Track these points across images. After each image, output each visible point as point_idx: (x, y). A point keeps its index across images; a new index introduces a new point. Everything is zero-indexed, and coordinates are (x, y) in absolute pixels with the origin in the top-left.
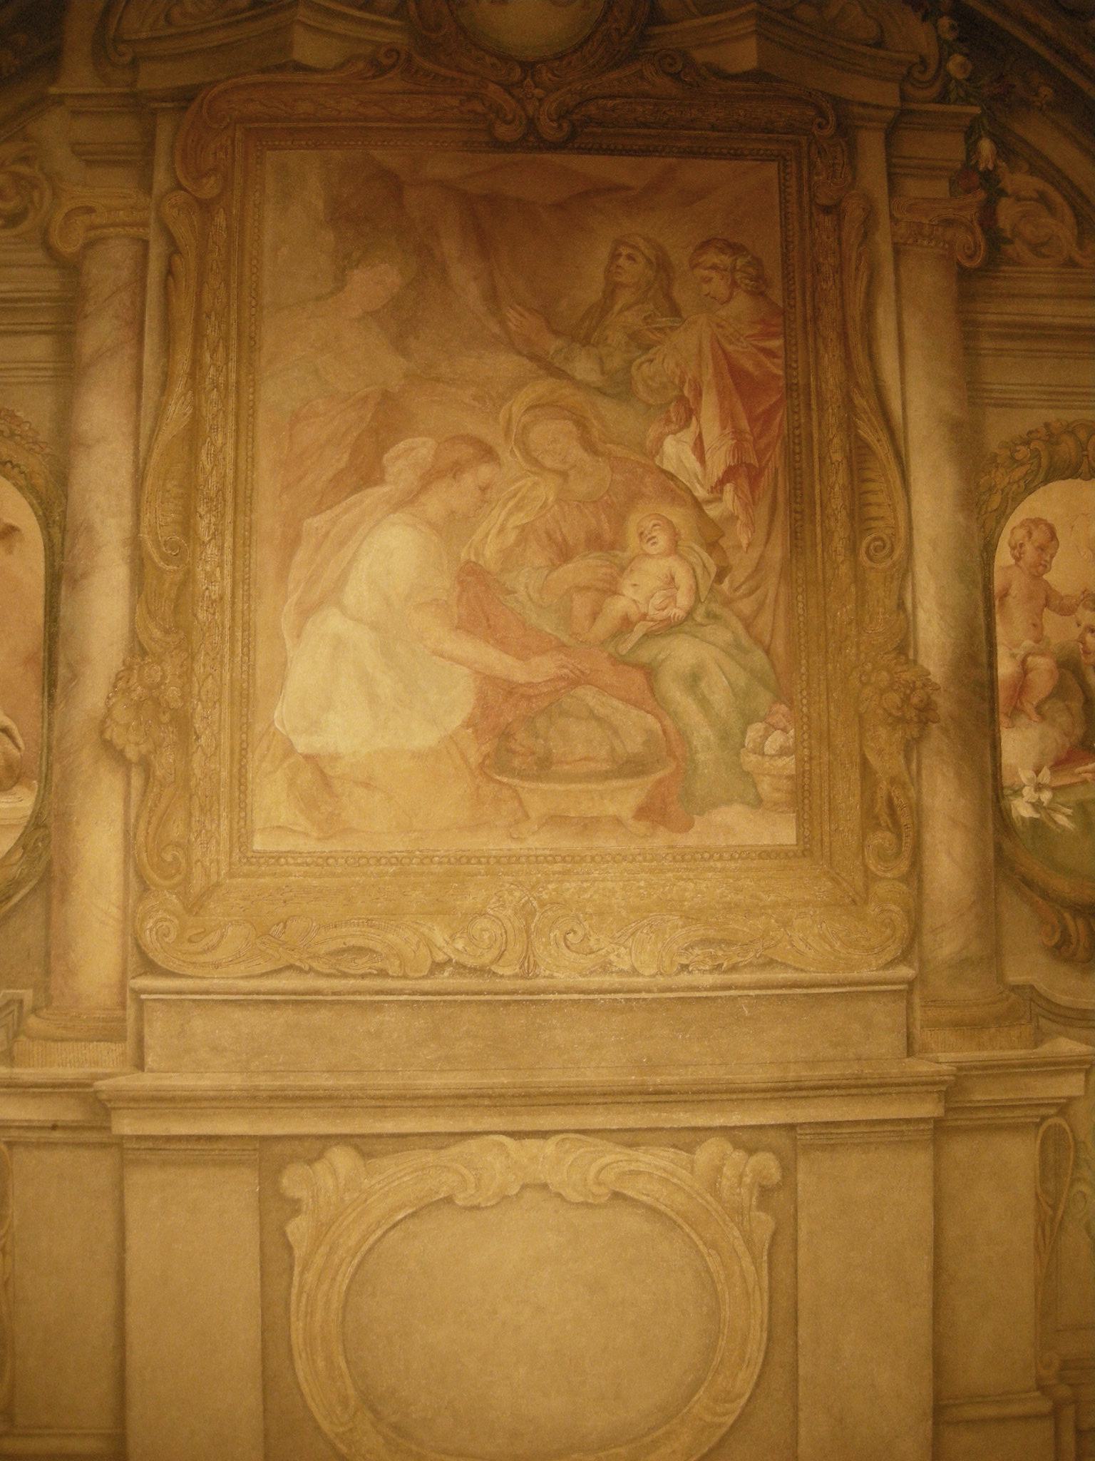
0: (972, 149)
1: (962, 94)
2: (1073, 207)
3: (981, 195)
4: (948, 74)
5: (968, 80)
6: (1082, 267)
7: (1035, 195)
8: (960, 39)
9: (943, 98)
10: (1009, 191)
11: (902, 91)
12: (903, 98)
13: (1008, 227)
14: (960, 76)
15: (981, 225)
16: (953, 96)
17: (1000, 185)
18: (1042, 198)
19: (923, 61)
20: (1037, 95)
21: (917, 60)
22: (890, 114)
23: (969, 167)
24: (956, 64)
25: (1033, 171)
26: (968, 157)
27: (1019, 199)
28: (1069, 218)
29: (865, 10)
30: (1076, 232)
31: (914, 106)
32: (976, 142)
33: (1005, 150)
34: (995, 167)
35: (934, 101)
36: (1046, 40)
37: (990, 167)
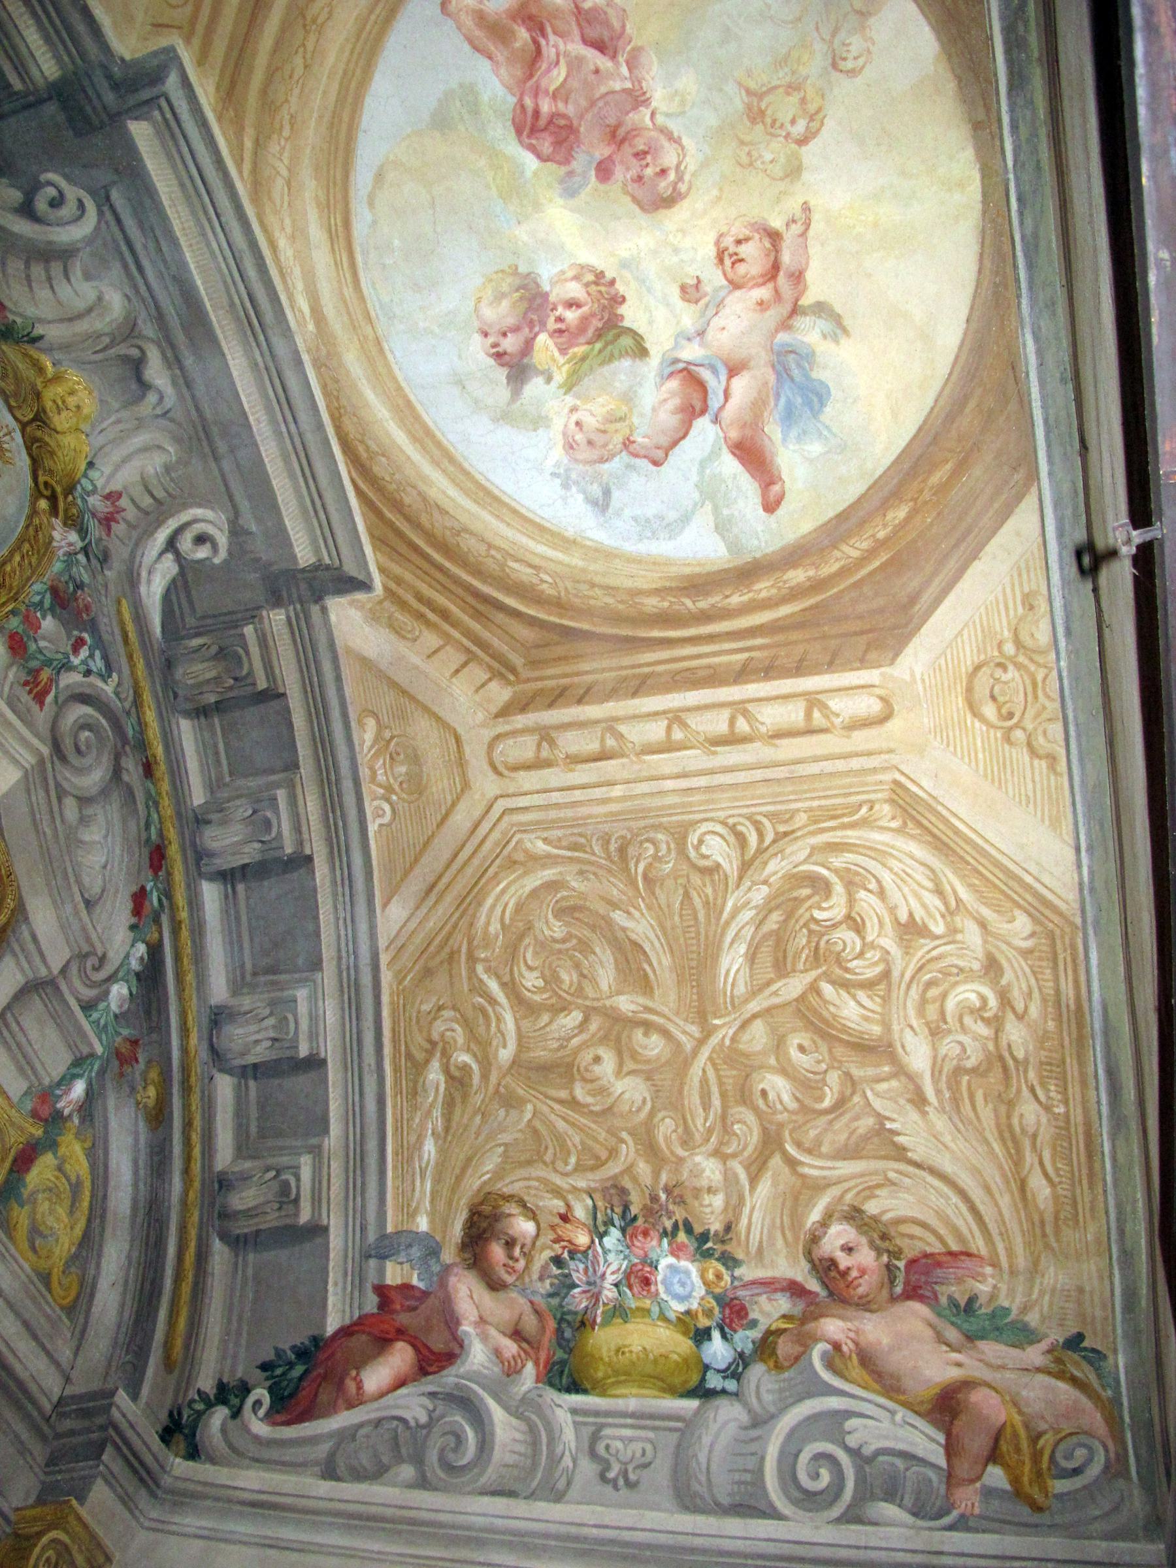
0: (67, 1080)
1: (102, 1022)
2: (89, 1221)
3: (38, 1132)
4: (107, 993)
5: (116, 1016)
6: (50, 1290)
7: (73, 1179)
8: (138, 975)
9: (88, 1007)
10: (62, 1150)
11: (68, 962)
12: (64, 970)
13: (30, 1187)
14: (114, 1007)
15: (15, 1161)
16: (95, 1015)
17: (59, 1139)
18: (76, 1188)
19: (103, 959)
20: (145, 1088)
21: (100, 954)
22: (43, 972)
23: (46, 1096)
24: (119, 991)
25: (90, 1153)
26: (59, 1084)
27: (60, 1169)
28: (78, 1231)
29: (105, 867)
30: (73, 1250)
31: (63, 987)
32: (75, 1077)
33: (88, 1108)
34: (70, 1116)
35: (78, 1000)
36: (185, 1050)
37: (66, 1112)
